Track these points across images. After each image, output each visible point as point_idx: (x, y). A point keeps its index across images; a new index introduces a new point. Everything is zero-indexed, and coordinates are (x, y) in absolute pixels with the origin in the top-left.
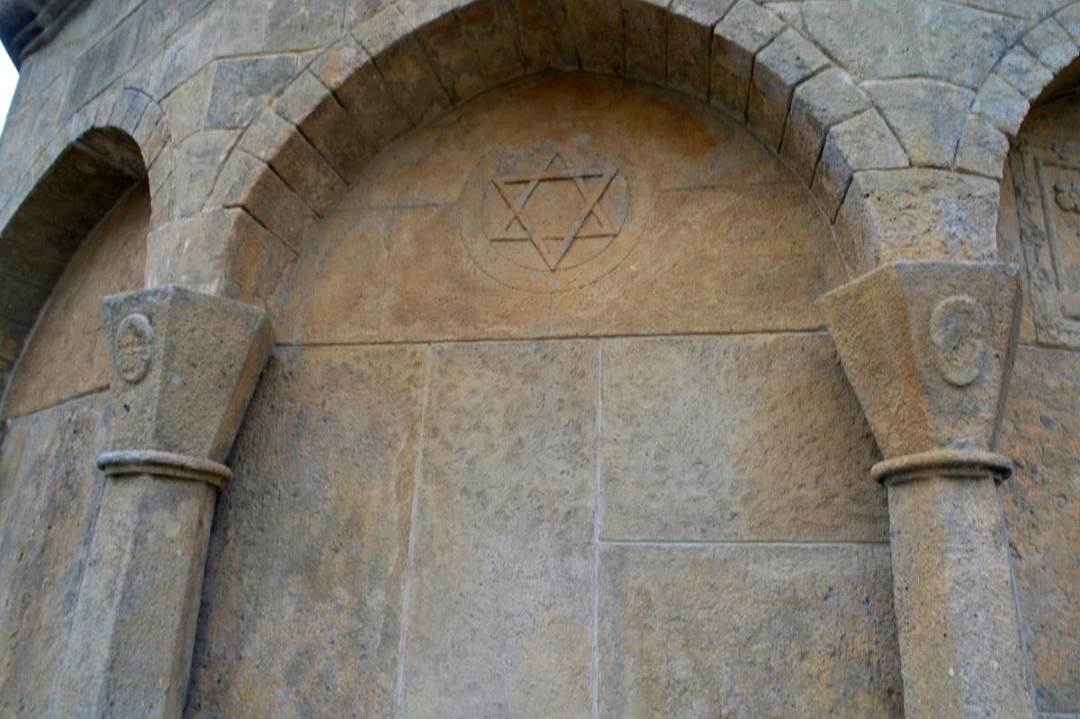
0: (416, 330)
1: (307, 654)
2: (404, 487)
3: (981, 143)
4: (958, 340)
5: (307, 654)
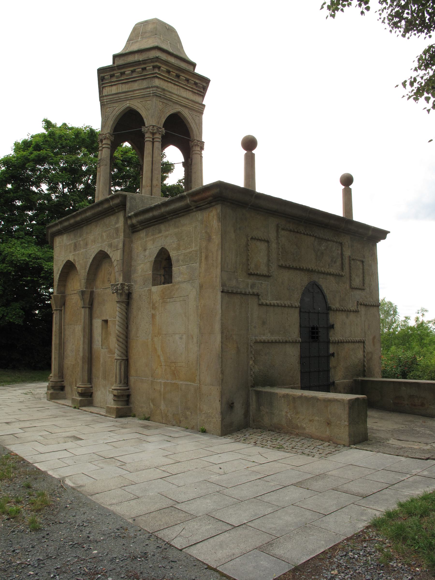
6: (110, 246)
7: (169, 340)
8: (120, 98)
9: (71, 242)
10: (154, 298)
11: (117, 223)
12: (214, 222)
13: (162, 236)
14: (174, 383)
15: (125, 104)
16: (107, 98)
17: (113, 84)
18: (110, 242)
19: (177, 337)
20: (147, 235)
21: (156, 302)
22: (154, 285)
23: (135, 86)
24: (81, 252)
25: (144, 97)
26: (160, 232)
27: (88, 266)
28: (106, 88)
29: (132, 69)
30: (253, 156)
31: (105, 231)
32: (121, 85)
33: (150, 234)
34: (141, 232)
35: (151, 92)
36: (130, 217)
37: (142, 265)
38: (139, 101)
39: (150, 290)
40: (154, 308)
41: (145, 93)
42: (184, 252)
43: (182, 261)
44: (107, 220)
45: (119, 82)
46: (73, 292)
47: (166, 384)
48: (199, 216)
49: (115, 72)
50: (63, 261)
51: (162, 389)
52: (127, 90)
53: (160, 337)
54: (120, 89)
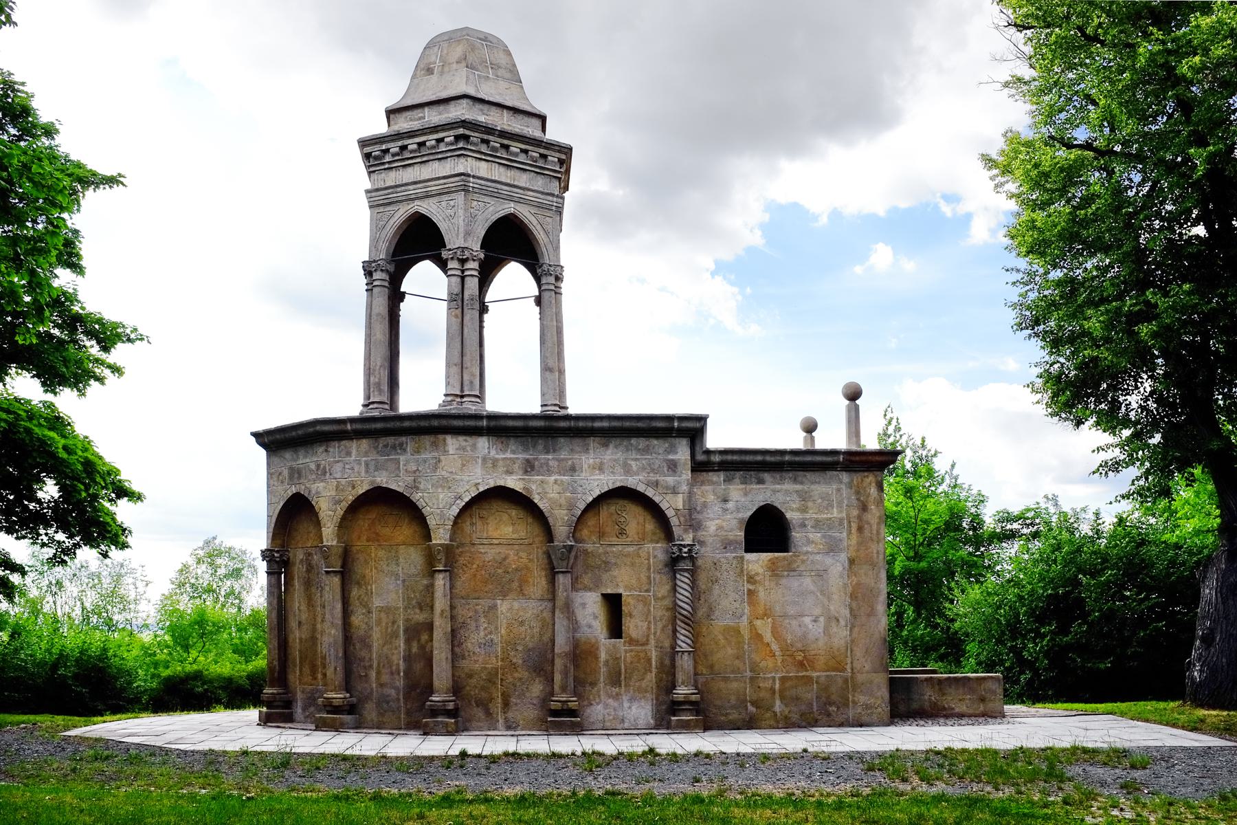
0: (370, 543)
1: (360, 596)
2: (371, 570)
3: (449, 519)
4: (438, 553)
5: (360, 596)
6: (656, 484)
7: (790, 624)
8: (500, 191)
9: (508, 455)
10: (750, 568)
11: (672, 449)
12: (872, 490)
13: (766, 488)
14: (803, 676)
15: (507, 206)
16: (474, 180)
17: (484, 157)
18: (654, 479)
19: (807, 620)
20: (728, 480)
21: (757, 574)
22: (747, 551)
23: (523, 180)
24: (553, 478)
25: (540, 206)
26: (761, 482)
27: (582, 506)
28: (469, 159)
29: (523, 147)
30: (857, 408)
31: (636, 460)
32: (497, 165)
33: (737, 480)
34: (710, 474)
35: (555, 204)
36: (708, 452)
37: (717, 521)
38: (532, 212)
39: (742, 558)
40: (751, 580)
41: (545, 202)
42: (814, 516)
43: (811, 527)
44: (642, 443)
45: (491, 158)
46: (485, 541)
47: (783, 679)
48: (845, 477)
49: (491, 138)
50: (477, 484)
51: (777, 686)
52: (509, 181)
53: (769, 620)
54: (497, 174)
